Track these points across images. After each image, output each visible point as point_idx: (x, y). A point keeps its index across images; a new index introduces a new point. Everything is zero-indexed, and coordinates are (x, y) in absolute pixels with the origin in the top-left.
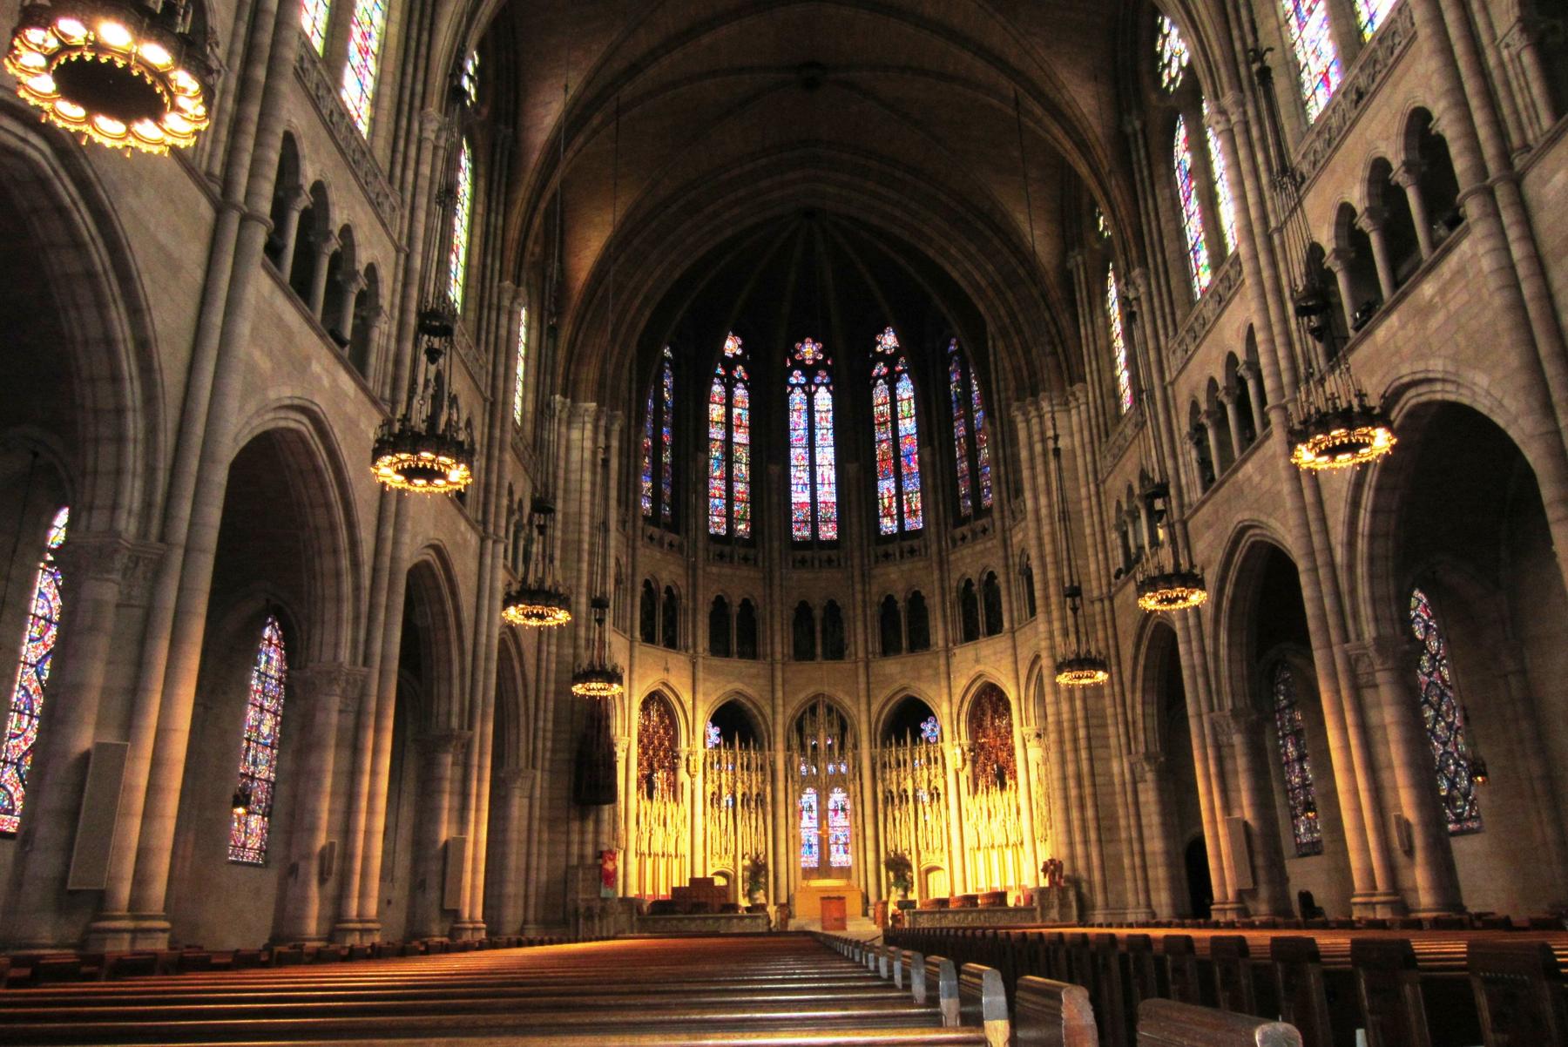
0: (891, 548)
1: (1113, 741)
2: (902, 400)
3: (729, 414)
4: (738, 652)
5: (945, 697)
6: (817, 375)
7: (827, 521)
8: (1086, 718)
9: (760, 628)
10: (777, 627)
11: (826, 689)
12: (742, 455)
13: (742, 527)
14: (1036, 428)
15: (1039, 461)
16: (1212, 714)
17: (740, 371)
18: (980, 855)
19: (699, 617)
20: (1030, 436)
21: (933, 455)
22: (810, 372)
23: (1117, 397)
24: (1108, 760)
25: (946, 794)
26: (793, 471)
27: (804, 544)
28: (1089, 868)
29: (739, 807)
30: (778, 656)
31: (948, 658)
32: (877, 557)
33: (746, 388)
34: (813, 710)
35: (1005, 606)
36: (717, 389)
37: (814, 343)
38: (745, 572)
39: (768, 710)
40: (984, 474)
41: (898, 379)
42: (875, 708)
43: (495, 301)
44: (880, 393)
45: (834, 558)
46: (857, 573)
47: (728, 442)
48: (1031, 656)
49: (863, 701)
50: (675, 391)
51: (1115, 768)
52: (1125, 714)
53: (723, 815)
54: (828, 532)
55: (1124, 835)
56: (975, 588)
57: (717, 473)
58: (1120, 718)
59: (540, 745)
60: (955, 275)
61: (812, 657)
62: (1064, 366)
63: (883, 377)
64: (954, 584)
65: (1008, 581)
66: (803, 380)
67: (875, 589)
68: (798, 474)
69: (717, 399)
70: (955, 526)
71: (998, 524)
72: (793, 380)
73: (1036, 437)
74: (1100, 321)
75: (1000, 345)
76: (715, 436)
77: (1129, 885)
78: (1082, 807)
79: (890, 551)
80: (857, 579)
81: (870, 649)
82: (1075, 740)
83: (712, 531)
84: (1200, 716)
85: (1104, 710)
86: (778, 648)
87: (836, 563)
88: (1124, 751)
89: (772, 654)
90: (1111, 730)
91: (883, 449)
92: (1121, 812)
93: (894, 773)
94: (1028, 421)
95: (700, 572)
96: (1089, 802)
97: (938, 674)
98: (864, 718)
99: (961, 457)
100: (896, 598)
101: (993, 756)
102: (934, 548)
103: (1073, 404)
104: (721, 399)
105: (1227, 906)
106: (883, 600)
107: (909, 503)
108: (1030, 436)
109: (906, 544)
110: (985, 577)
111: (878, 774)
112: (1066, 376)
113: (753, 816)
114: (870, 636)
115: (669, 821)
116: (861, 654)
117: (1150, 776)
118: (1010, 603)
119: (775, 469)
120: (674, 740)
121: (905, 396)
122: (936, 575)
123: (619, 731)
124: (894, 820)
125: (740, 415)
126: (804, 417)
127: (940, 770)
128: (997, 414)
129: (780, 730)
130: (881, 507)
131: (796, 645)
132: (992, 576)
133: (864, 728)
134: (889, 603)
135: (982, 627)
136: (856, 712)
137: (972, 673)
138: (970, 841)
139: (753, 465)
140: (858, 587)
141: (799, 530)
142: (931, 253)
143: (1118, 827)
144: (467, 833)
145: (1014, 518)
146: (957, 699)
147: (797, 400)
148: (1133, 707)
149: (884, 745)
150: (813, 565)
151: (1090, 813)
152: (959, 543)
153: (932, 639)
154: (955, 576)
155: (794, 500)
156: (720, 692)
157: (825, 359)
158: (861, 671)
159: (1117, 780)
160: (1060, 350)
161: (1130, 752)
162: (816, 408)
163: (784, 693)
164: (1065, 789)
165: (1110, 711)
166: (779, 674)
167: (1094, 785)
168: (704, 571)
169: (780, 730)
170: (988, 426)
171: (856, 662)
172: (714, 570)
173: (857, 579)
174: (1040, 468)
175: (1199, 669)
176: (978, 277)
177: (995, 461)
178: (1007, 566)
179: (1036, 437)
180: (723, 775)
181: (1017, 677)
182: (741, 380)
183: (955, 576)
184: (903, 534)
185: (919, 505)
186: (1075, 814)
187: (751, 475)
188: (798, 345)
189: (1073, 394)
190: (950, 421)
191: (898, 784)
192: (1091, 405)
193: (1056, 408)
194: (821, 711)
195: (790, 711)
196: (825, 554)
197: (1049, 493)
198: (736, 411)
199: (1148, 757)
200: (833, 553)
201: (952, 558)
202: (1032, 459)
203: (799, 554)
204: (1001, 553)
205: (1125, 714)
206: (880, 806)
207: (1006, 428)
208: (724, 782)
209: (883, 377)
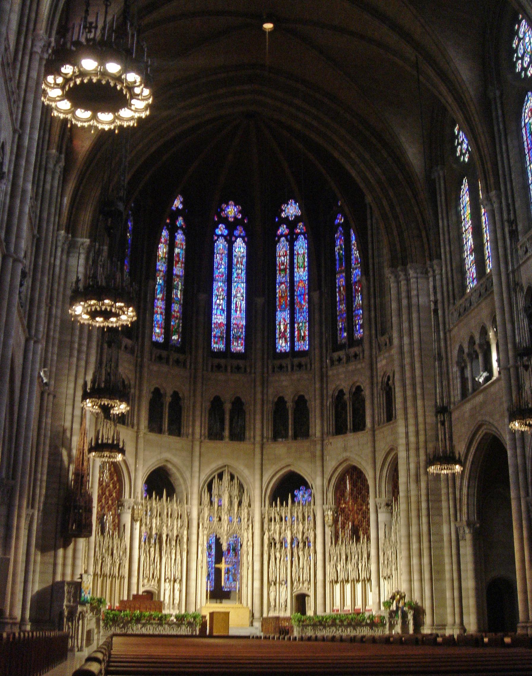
0: (284, 362)
1: (445, 512)
4: (169, 429)
5: (319, 473)
6: (236, 229)
7: (238, 338)
8: (428, 495)
9: (184, 414)
10: (198, 413)
12: (179, 283)
13: (175, 337)
14: (403, 288)
15: (404, 311)
16: (528, 498)
17: (180, 221)
18: (337, 587)
20: (399, 293)
21: (321, 297)
22: (231, 226)
23: (462, 272)
24: (440, 524)
25: (315, 542)
27: (219, 354)
28: (422, 598)
29: (164, 544)
30: (197, 436)
31: (322, 445)
32: (273, 368)
33: (184, 233)
34: (221, 476)
35: (368, 412)
36: (165, 233)
37: (235, 206)
40: (358, 315)
41: (296, 239)
42: (266, 479)
43: (44, 163)
44: (282, 248)
46: (258, 378)
47: (169, 276)
48: (387, 449)
50: (134, 232)
51: (445, 529)
52: (454, 493)
53: (152, 549)
54: (238, 347)
55: (448, 576)
56: (346, 397)
57: (160, 296)
58: (451, 496)
59: (38, 491)
60: (354, 174)
62: (426, 246)
63: (286, 236)
64: (330, 393)
65: (372, 394)
66: (226, 232)
67: (271, 391)
68: (218, 301)
70: (334, 350)
71: (367, 353)
72: (218, 232)
73: (404, 295)
74: (454, 218)
75: (382, 226)
76: (160, 268)
77: (449, 610)
78: (420, 556)
79: (284, 365)
80: (258, 383)
81: (265, 435)
82: (419, 510)
83: (154, 339)
84: (519, 499)
85: (440, 489)
86: (198, 430)
87: (243, 370)
88: (452, 518)
89: (193, 434)
90: (444, 504)
91: (281, 289)
92: (447, 560)
93: (278, 526)
94: (398, 282)
95: (146, 370)
96: (426, 553)
97: (314, 456)
98: (257, 484)
99: (340, 301)
100: (286, 399)
101: (351, 517)
102: (317, 365)
103: (431, 274)
104: (166, 241)
105: (528, 625)
106: (276, 400)
107: (299, 330)
108: (399, 293)
109: (296, 361)
110: (354, 390)
111: (266, 526)
112: (427, 254)
113: (174, 551)
115: (115, 552)
116: (258, 438)
117: (468, 536)
118: (373, 410)
119: (202, 297)
120: (120, 493)
121: (301, 251)
122: (318, 386)
124: (276, 559)
125: (179, 254)
126: (225, 260)
127: (312, 525)
128: (371, 274)
129: (195, 490)
130: (278, 331)
131: (210, 429)
132: (359, 389)
134: (280, 403)
135: (349, 425)
137: (341, 458)
138: (330, 576)
139: (185, 292)
141: (217, 343)
142: (336, 155)
143: (443, 571)
144: (9, 554)
145: (380, 350)
146: (327, 476)
147: (221, 247)
148: (461, 489)
149: (271, 505)
150: (226, 370)
151: (426, 560)
152: (336, 363)
153: (311, 431)
154: (332, 387)
155: (214, 321)
156: (154, 460)
157: (243, 218)
158: (258, 450)
159: (446, 538)
160: (424, 234)
161: (456, 520)
162: (234, 254)
164: (409, 543)
165: (444, 491)
166: (197, 449)
167: (430, 541)
168: (148, 368)
170: (364, 282)
171: (254, 444)
172: (155, 368)
173: (258, 383)
174: (405, 317)
175: (520, 468)
176: (368, 175)
177: (367, 307)
178: (372, 383)
179: (404, 295)
180: (154, 521)
181: (374, 462)
182: (181, 227)
183: (332, 387)
184: (293, 353)
185: (307, 333)
186: (415, 561)
189: (432, 267)
190: (333, 274)
191: (280, 534)
192: (444, 276)
193: (419, 275)
194: (226, 477)
195: (203, 477)
196: (235, 362)
197: (411, 335)
198: (177, 250)
199: (469, 524)
200: (241, 363)
201: (330, 373)
202: (400, 309)
203: (216, 361)
204: (368, 373)
205: (454, 493)
206: (266, 548)
207: (377, 284)
208: (154, 525)
209: (286, 236)
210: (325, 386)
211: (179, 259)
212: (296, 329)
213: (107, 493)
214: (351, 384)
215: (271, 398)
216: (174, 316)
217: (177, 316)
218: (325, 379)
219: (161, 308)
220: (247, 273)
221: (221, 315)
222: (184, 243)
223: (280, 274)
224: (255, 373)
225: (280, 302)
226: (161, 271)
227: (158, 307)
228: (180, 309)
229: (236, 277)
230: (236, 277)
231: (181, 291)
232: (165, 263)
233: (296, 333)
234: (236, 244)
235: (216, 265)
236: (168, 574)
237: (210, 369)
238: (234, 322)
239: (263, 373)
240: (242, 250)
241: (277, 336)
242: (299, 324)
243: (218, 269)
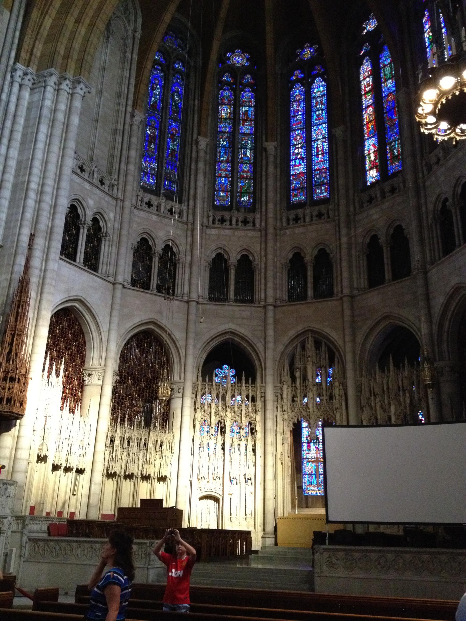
2: (385, 66)
3: (235, 112)
7: (323, 184)
11: (317, 326)
13: (245, 199)
26: (292, 149)
30: (270, 300)
33: (253, 91)
39: (260, 347)
45: (324, 211)
46: (343, 219)
49: (348, 332)
57: (224, 158)
61: (303, 297)
64: (431, 207)
67: (360, 230)
68: (296, 151)
69: (226, 101)
86: (270, 292)
87: (326, 216)
104: (230, 101)
106: (368, 240)
107: (392, 151)
113: (243, 443)
115: (151, 445)
116: (346, 291)
123: (96, 361)
125: (246, 111)
126: (302, 105)
130: (367, 161)
133: (349, 358)
139: (254, 150)
140: (344, 231)
141: (296, 196)
146: (436, 320)
155: (293, 172)
156: (213, 333)
163: (275, 331)
169: (269, 364)
171: (341, 299)
172: (214, 231)
173: (342, 225)
182: (248, 85)
187: (255, 158)
188: (299, 51)
195: (281, 348)
208: (213, 411)
210: (423, 201)
211: (248, 115)
212: (388, 151)
214: (453, 182)
216: (242, 177)
217: (247, 176)
218: (422, 193)
219: (226, 170)
220: (327, 112)
221: (300, 164)
222: (253, 100)
223: (366, 98)
224: (339, 215)
225: (368, 128)
226: (225, 133)
227: (221, 170)
228: (251, 168)
229: (316, 120)
230: (316, 120)
231: (251, 149)
232: (229, 124)
233: (389, 155)
234: (314, 86)
235: (292, 114)
236: (235, 474)
237: (285, 223)
238: (316, 167)
240: (322, 89)
241: (367, 167)
242: (391, 143)
243: (295, 117)
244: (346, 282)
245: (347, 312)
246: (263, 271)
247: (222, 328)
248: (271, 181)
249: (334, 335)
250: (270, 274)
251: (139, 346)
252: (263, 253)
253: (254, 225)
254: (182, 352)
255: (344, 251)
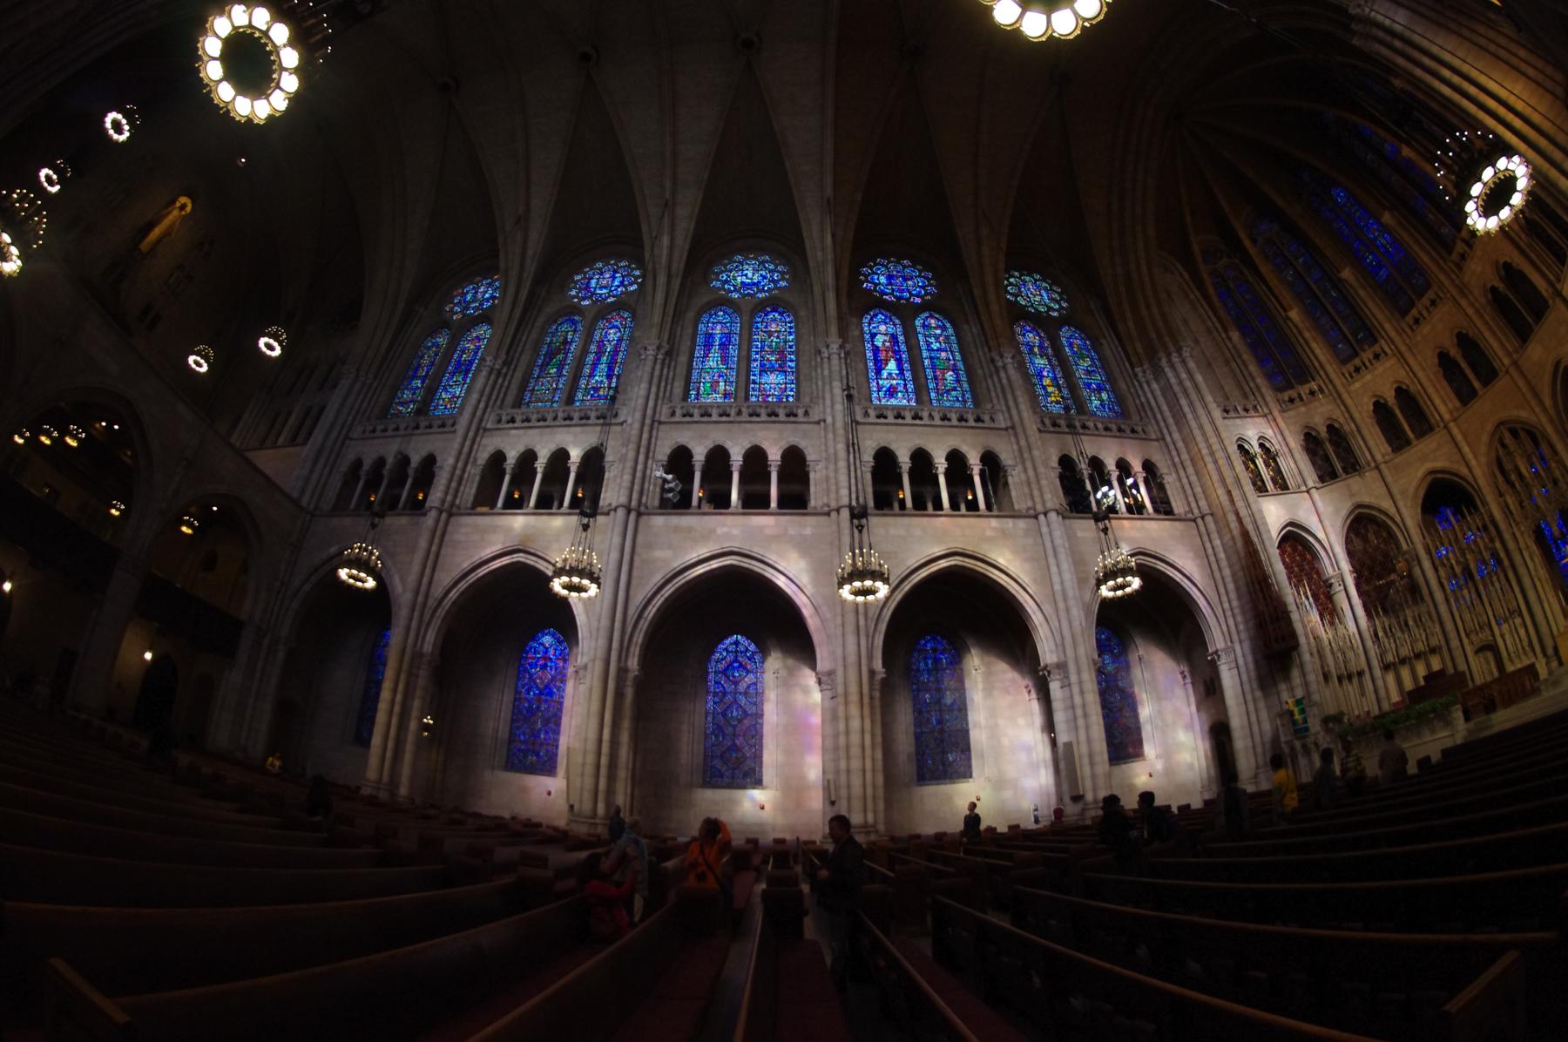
19: (1365, 432)
38: (1380, 368)
49: (1533, 402)
79: (1462, 251)
81: (1511, 350)
86: (1442, 409)
114: (1504, 341)
116: (1506, 361)
136: (1536, 419)
140: (1464, 303)
158: (1516, 375)
171: (1507, 372)
173: (1458, 297)
213: (1380, 558)
215: (1483, 300)
239: (1453, 281)
244: (1501, 353)
245: (1521, 383)
246: (1422, 391)
247: (1420, 473)
248: (1371, 304)
249: (1524, 414)
250: (1431, 390)
251: (1357, 535)
252: (1411, 374)
253: (1386, 354)
254: (1398, 519)
255: (1479, 323)
